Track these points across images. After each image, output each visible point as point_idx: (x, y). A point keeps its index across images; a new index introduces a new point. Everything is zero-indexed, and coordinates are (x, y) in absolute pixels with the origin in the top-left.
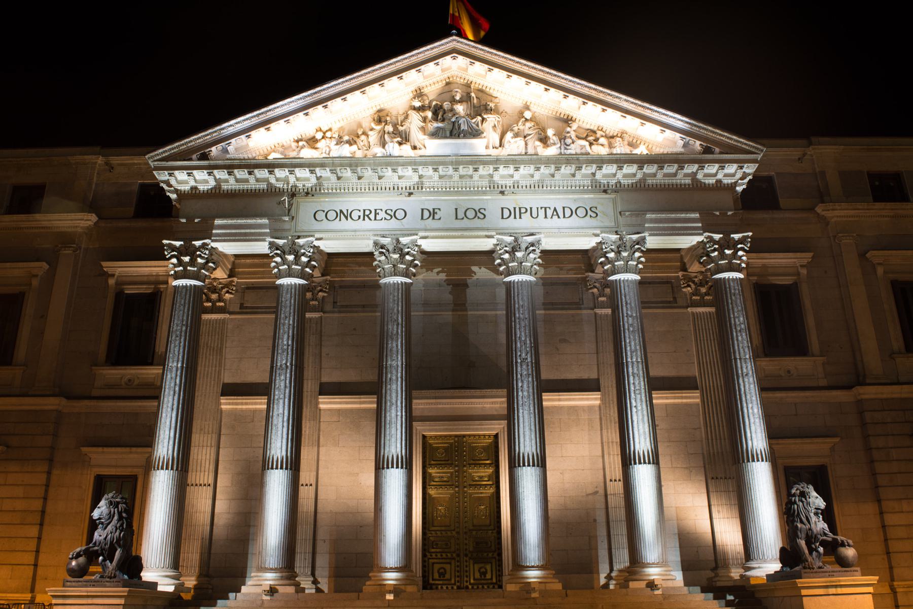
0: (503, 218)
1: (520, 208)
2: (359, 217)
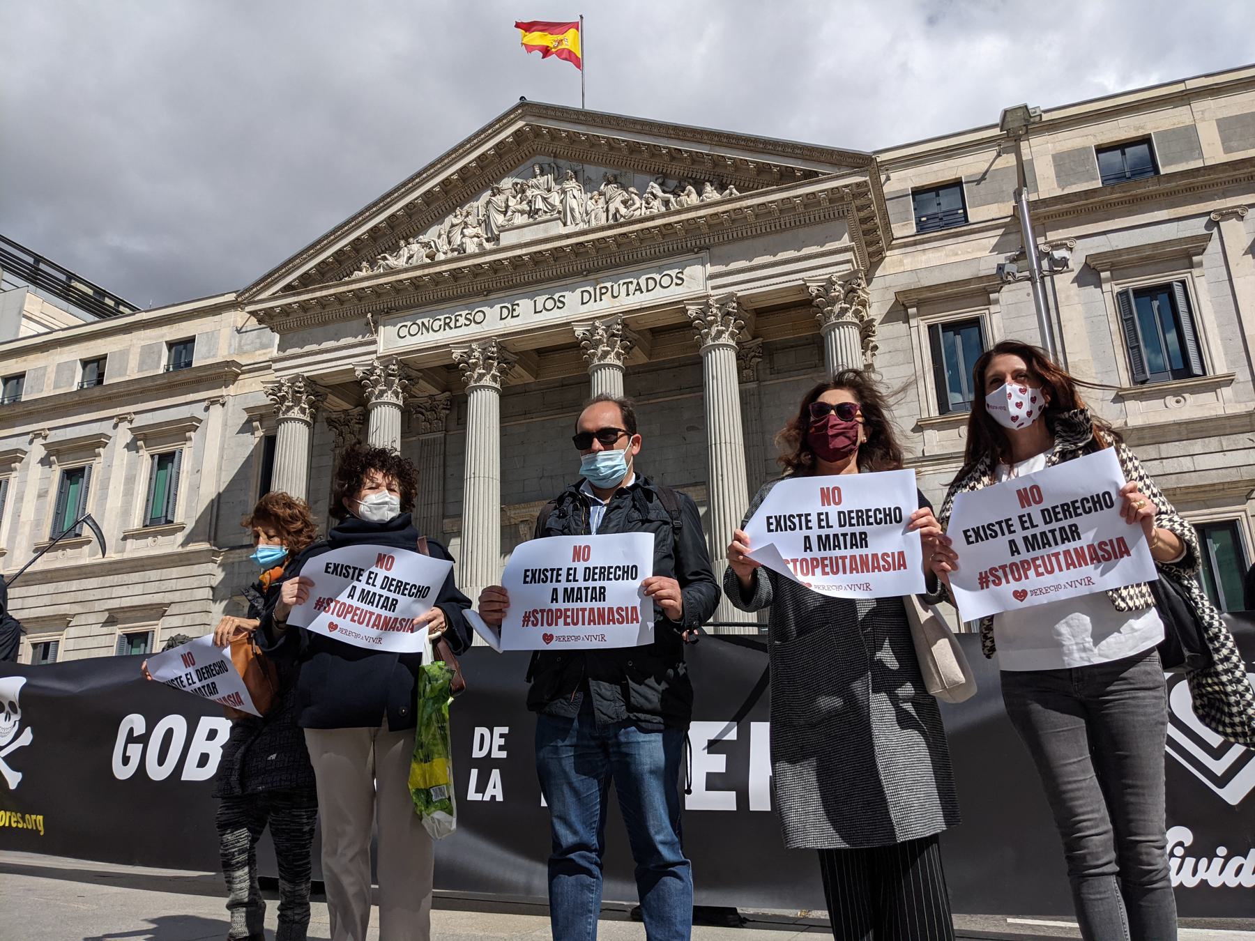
2: (440, 326)
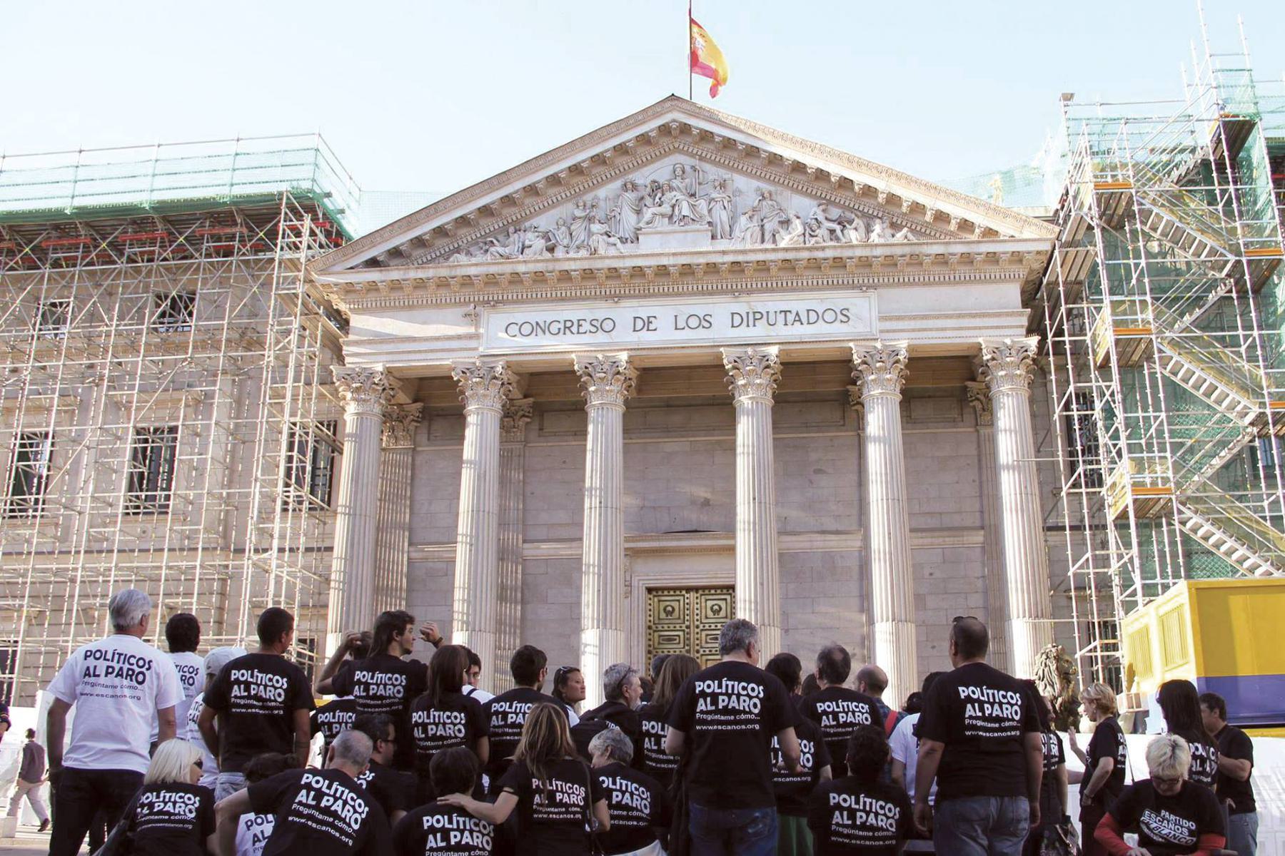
0: (733, 326)
1: (754, 313)
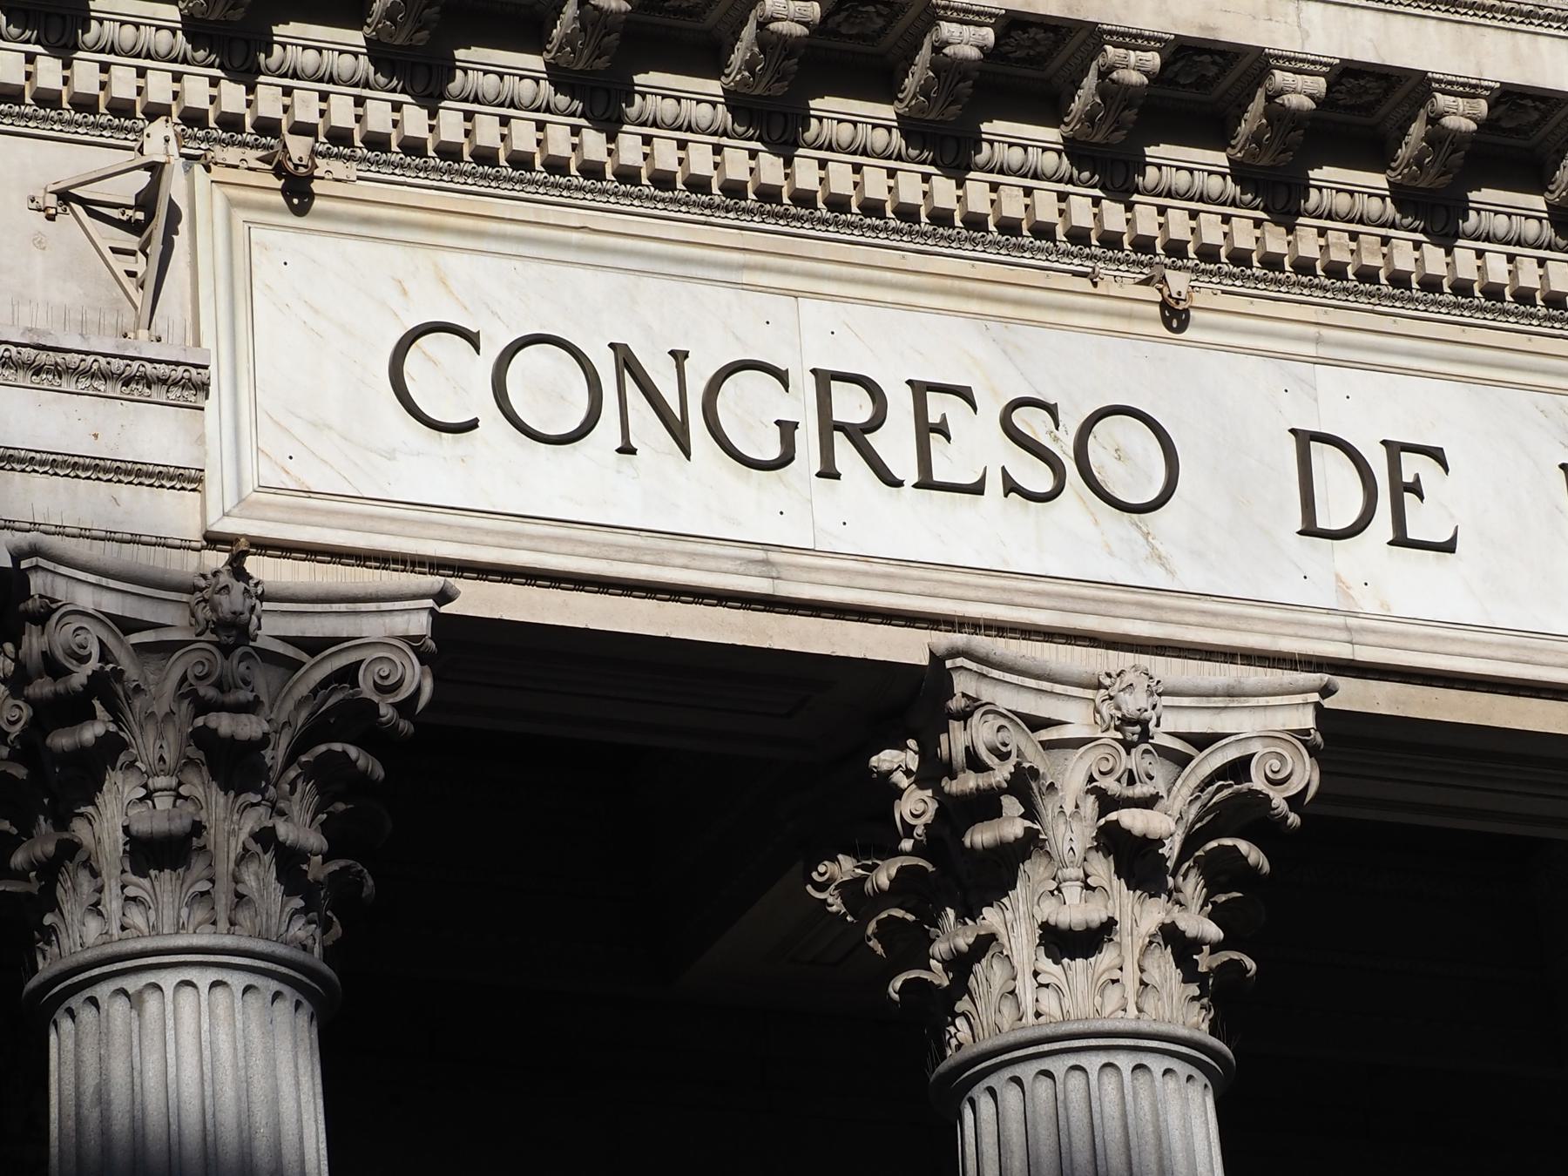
2: (787, 429)
